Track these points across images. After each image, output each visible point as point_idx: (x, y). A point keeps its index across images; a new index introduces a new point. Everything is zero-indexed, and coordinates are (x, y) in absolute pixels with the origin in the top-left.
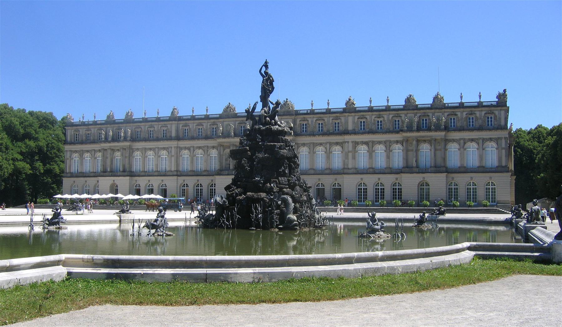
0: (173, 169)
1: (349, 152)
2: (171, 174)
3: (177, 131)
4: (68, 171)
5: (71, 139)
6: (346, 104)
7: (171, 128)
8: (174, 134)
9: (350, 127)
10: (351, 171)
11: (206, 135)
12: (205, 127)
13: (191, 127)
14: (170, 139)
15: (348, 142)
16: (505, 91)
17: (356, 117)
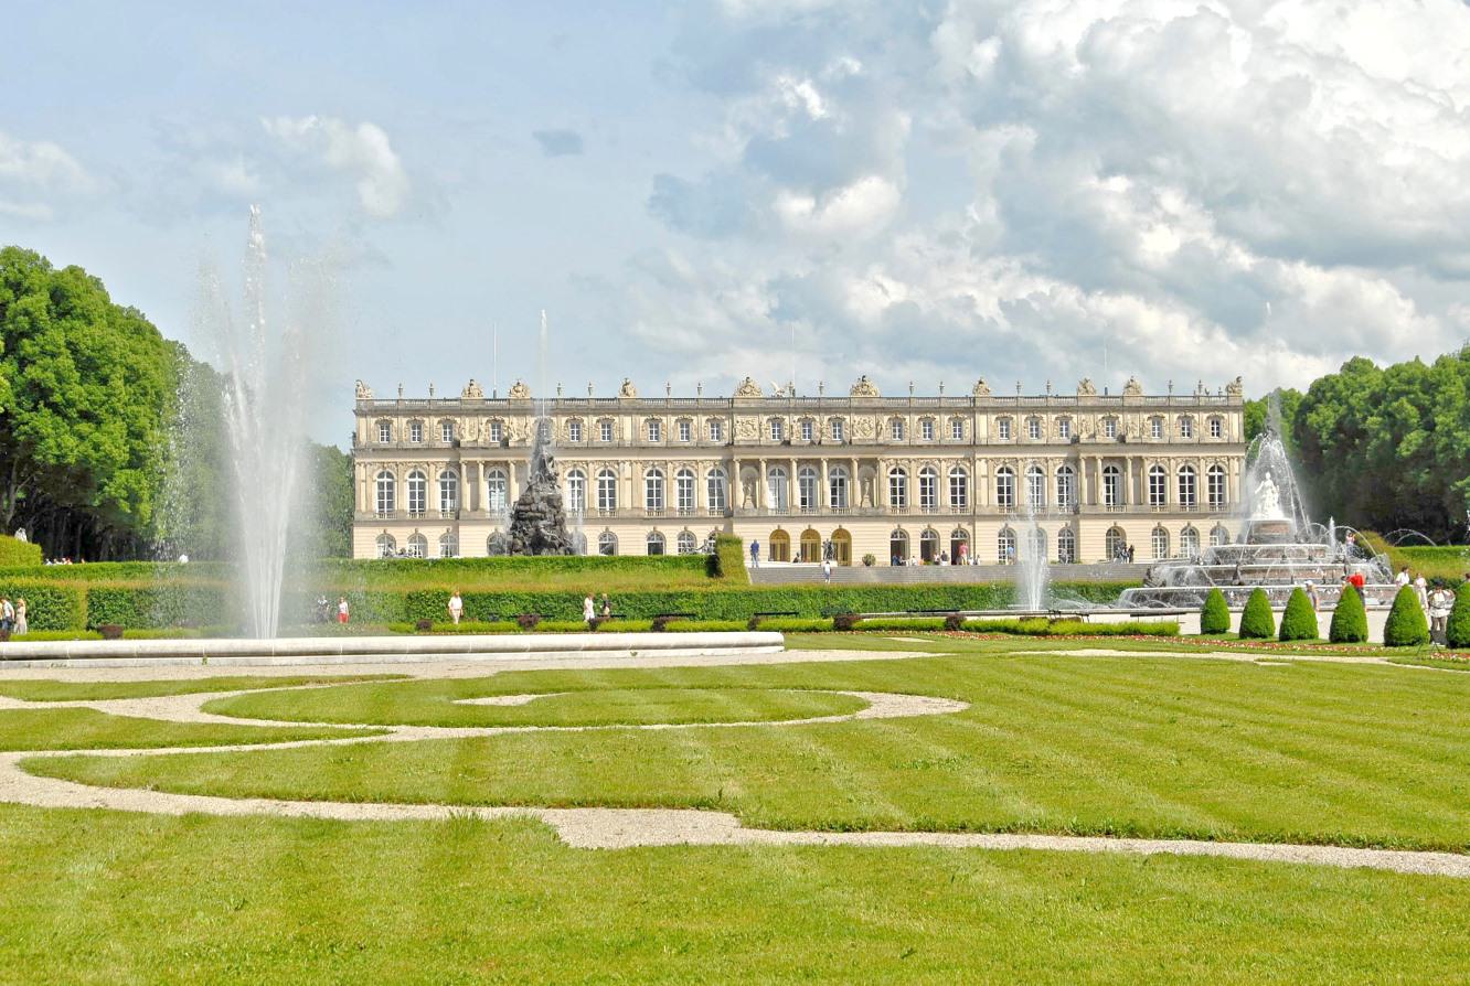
0: (628, 506)
1: (983, 476)
2: (626, 515)
3: (634, 427)
4: (363, 508)
5: (368, 436)
6: (976, 390)
7: (621, 422)
8: (628, 435)
9: (983, 432)
10: (987, 513)
11: (700, 440)
12: (695, 422)
13: (665, 421)
14: (620, 448)
15: (980, 460)
16: (1238, 380)
17: (994, 417)
